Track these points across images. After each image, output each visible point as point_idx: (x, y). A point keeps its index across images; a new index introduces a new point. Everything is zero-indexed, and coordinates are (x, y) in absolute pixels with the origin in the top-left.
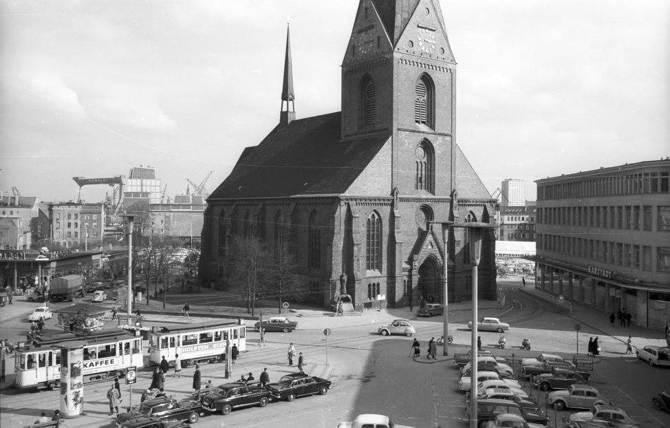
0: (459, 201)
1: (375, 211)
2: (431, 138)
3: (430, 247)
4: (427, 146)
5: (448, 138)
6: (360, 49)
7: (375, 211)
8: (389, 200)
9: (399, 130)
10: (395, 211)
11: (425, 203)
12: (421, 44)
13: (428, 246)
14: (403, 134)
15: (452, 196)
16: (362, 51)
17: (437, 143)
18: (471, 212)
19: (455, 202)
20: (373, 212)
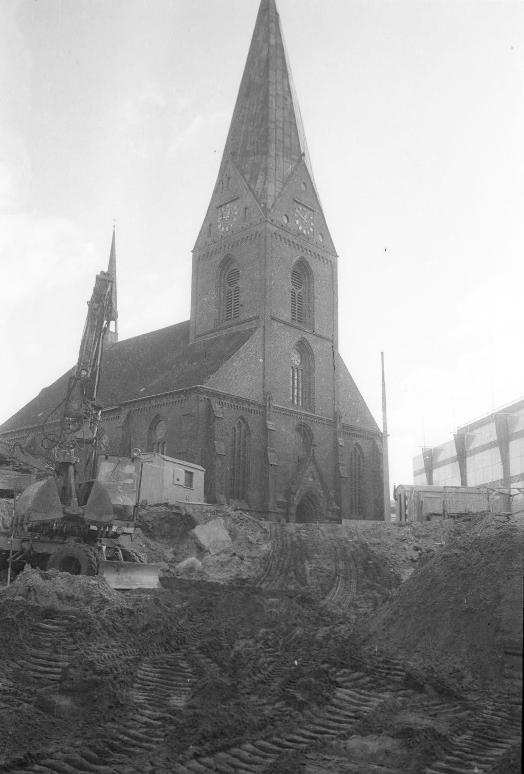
0: (343, 427)
1: (242, 418)
2: (310, 338)
3: (310, 479)
4: (303, 348)
5: (329, 344)
6: (219, 226)
7: (242, 418)
8: (260, 406)
9: (273, 318)
10: (268, 422)
11: (307, 422)
12: (297, 222)
13: (308, 477)
14: (276, 325)
15: (335, 418)
16: (221, 228)
17: (316, 347)
18: (357, 444)
19: (339, 426)
20: (240, 420)
